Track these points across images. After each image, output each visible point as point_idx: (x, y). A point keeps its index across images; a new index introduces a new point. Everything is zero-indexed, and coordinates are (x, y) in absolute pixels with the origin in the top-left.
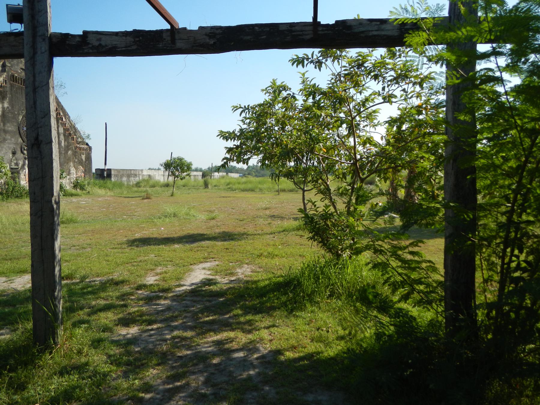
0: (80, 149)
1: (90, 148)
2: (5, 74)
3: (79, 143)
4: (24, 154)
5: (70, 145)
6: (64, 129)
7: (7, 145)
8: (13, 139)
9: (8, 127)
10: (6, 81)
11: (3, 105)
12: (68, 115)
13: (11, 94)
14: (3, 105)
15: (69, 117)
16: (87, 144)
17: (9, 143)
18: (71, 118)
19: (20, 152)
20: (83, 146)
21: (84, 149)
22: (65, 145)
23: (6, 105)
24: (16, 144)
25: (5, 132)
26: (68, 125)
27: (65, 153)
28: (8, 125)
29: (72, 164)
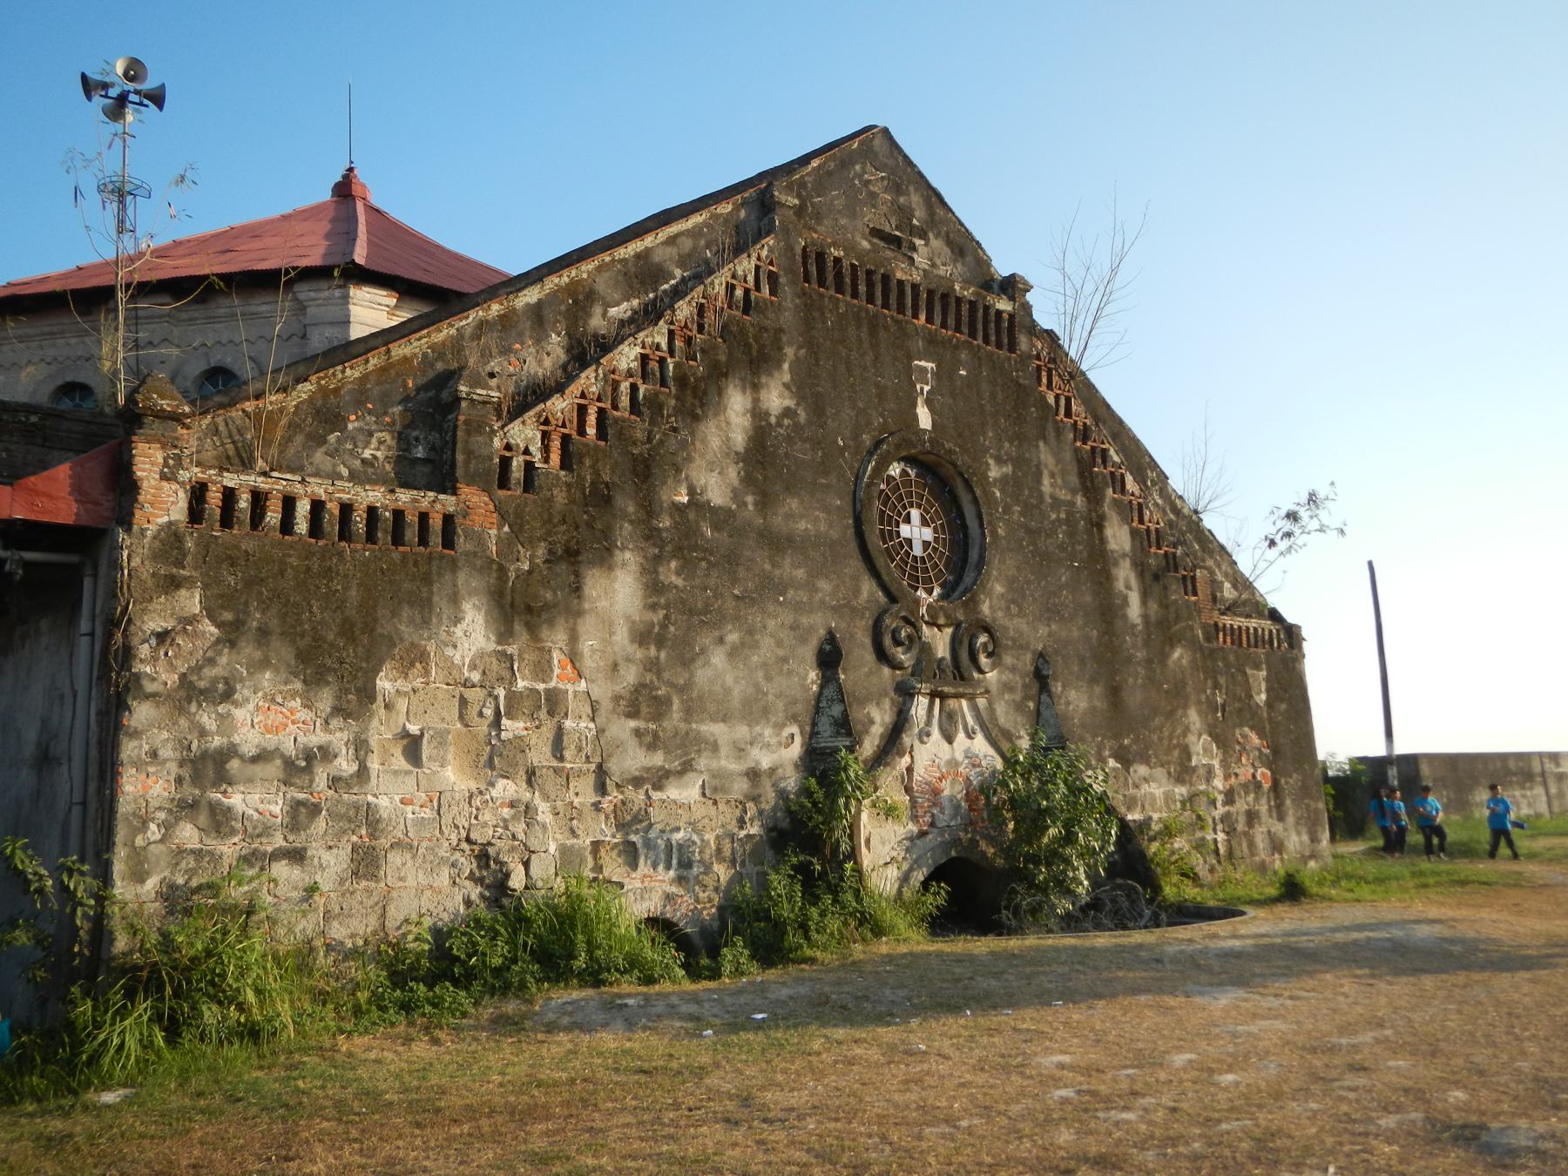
0: (1236, 634)
1: (1292, 635)
2: (770, 241)
3: (1231, 609)
4: (895, 666)
5: (1178, 618)
6: (1134, 533)
7: (788, 617)
8: (825, 585)
9: (789, 516)
10: (772, 277)
11: (756, 401)
12: (1154, 465)
13: (811, 345)
14: (756, 401)
15: (1163, 478)
16: (1274, 615)
17: (798, 608)
18: (1177, 483)
19: (869, 656)
20: (1253, 623)
21: (1258, 640)
22: (1145, 617)
23: (776, 399)
24: (846, 608)
25: (777, 543)
26: (1154, 518)
27: (1149, 662)
28: (793, 503)
29: (1194, 718)
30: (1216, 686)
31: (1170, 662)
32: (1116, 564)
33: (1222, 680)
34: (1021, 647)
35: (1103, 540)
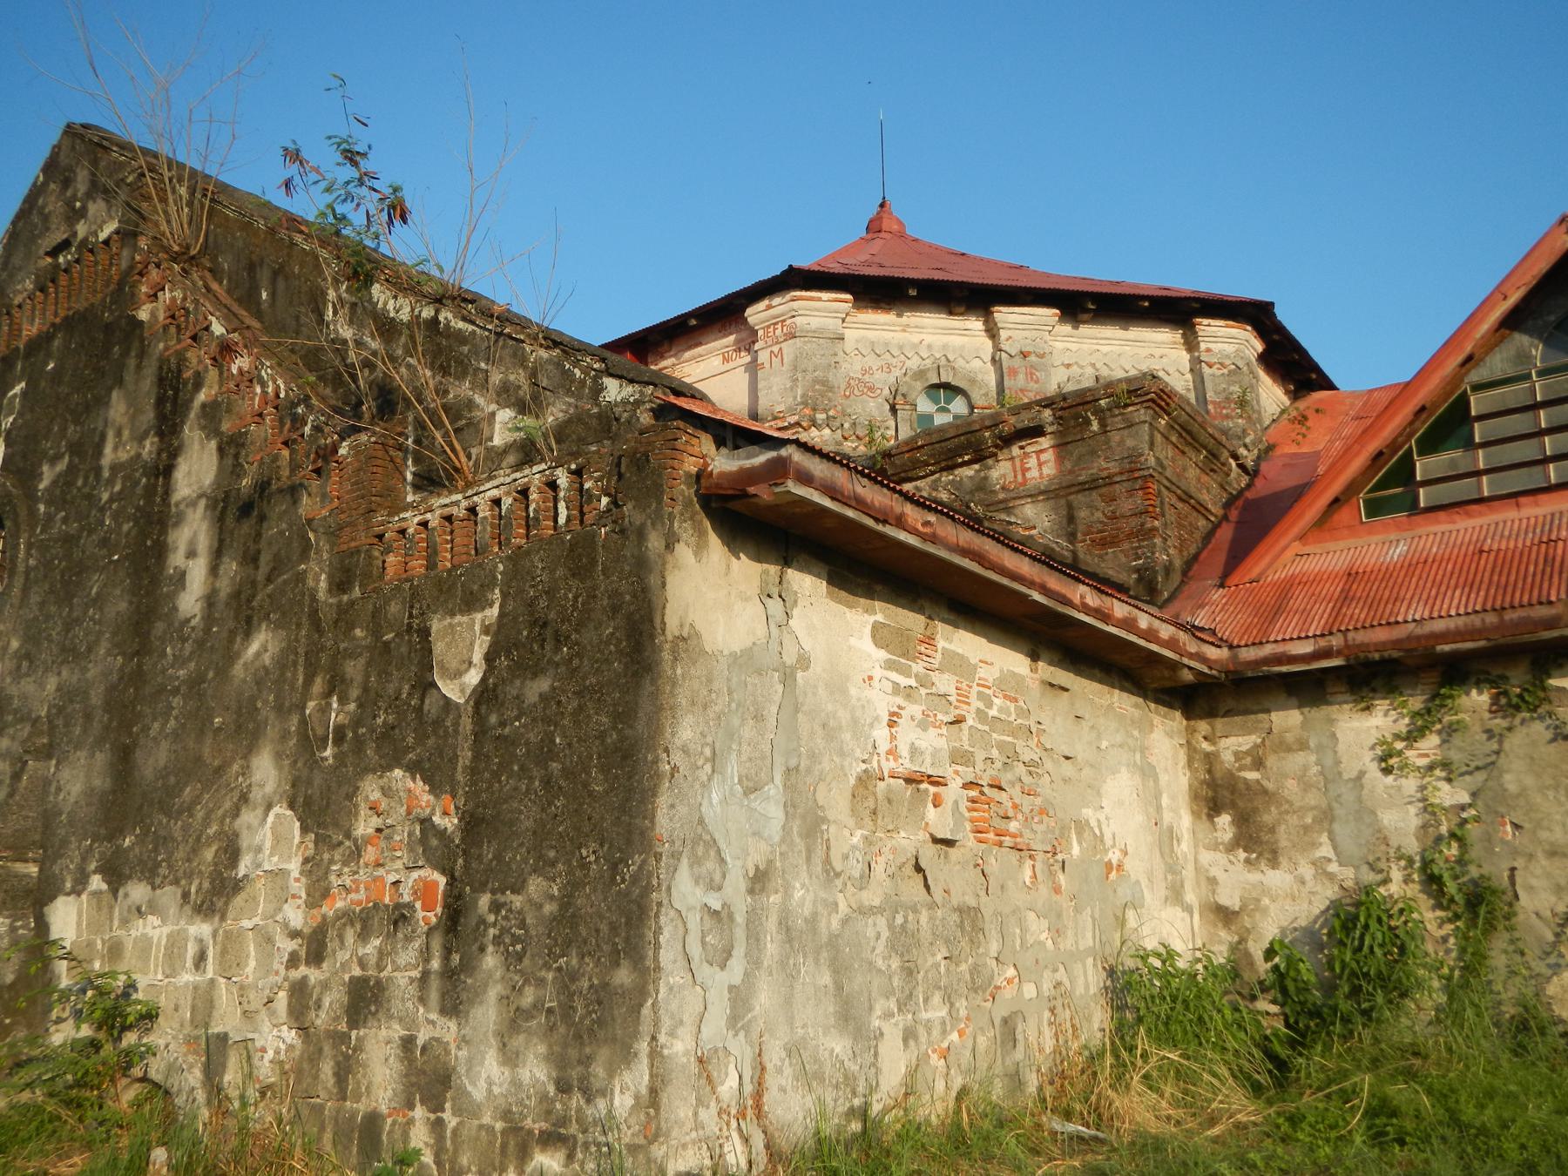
27: (196, 681)
29: (266, 771)
30: (337, 685)
31: (238, 670)
32: (180, 519)
33: (353, 669)
34: (22, 720)
35: (167, 492)
